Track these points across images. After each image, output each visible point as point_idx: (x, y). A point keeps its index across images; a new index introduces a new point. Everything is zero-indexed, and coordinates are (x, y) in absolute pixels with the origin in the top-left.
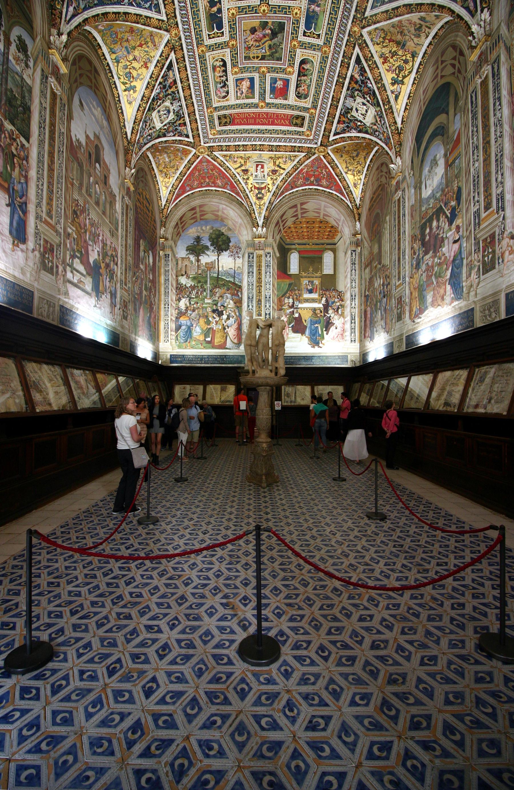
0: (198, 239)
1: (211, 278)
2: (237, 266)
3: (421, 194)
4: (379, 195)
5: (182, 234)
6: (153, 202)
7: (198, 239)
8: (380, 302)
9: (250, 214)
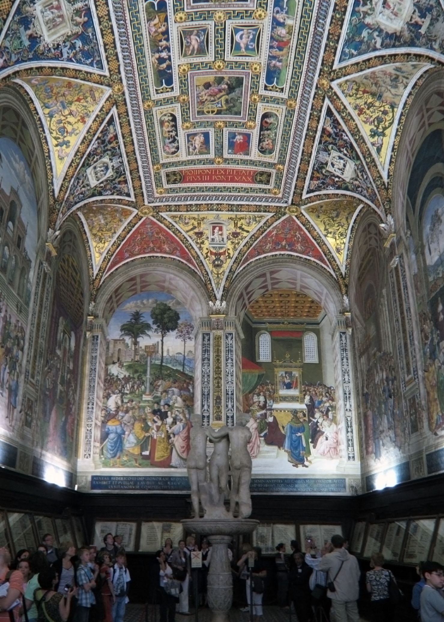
1: (153, 366)
2: (187, 351)
4: (369, 261)
5: (117, 310)
7: (137, 316)
8: (385, 403)
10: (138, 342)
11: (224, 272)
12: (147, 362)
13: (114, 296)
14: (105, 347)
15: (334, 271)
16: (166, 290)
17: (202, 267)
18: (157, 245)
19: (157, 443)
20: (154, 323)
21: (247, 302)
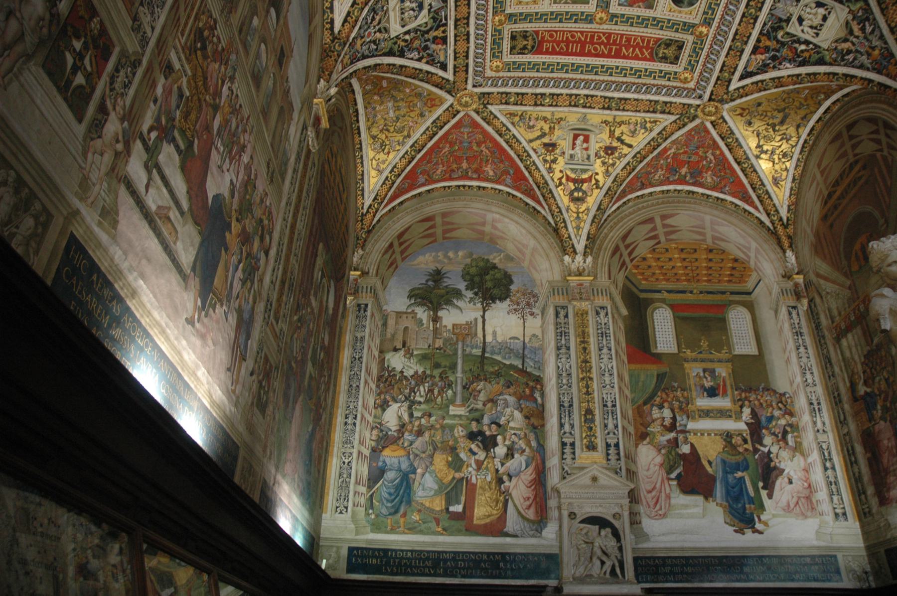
0: (437, 276)
1: (467, 357)
2: (529, 333)
7: (437, 276)
11: (588, 209)
12: (456, 350)
13: (396, 244)
14: (380, 324)
15: (768, 215)
16: (488, 237)
17: (552, 201)
19: (478, 491)
21: (627, 260)
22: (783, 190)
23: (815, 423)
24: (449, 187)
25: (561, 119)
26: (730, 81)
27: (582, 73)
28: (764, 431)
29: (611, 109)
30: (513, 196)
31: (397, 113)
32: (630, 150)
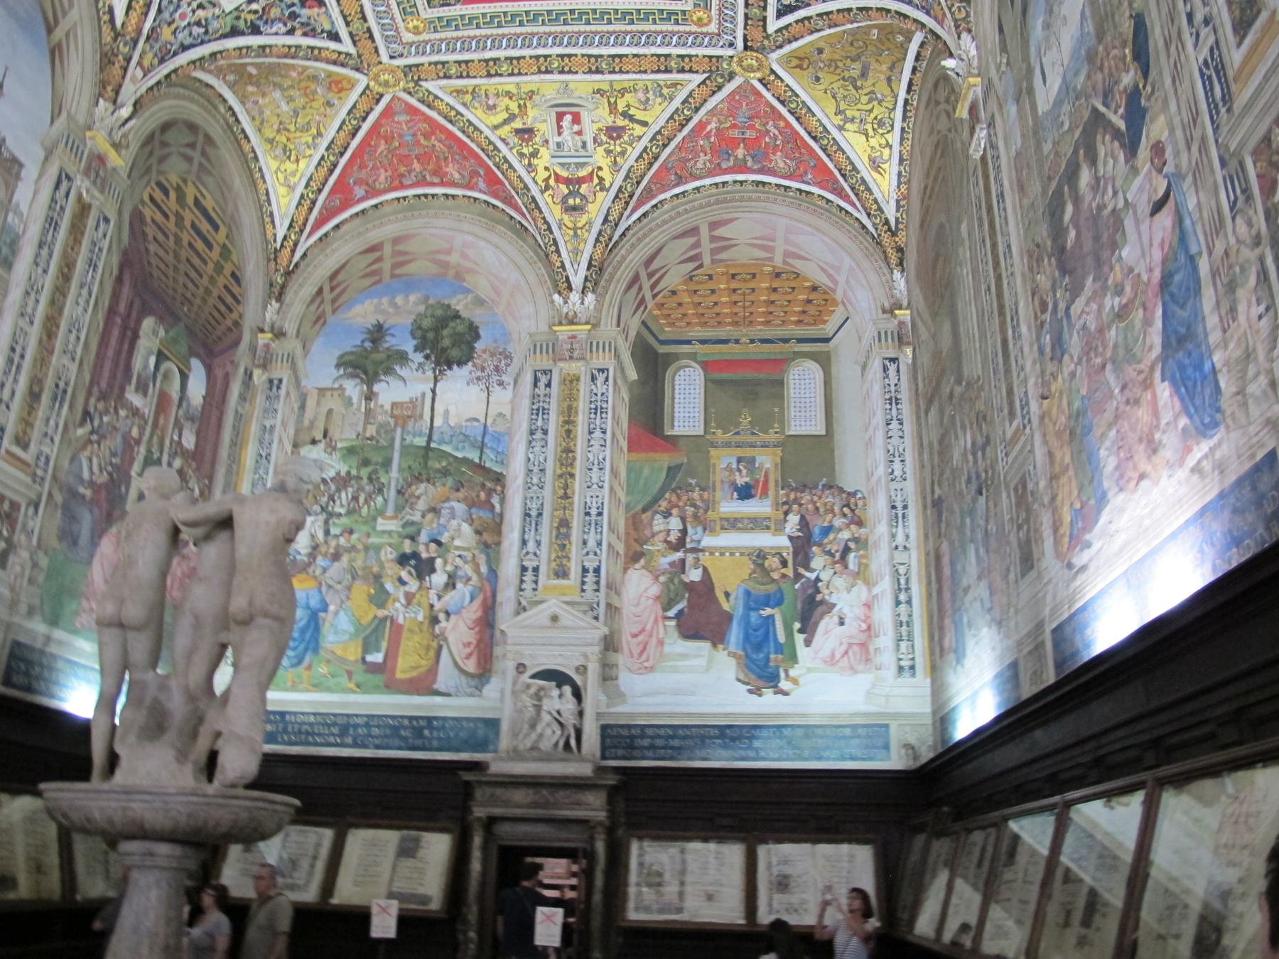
2: (493, 411)
3: (1034, 107)
5: (331, 319)
6: (233, 225)
7: (378, 333)
9: (547, 254)
10: (376, 395)
12: (393, 440)
14: (296, 406)
15: (869, 215)
16: (452, 272)
18: (431, 167)
19: (405, 634)
20: (417, 349)
21: (648, 296)
22: (887, 176)
23: (893, 536)
24: (404, 198)
25: (533, 92)
26: (764, 19)
27: (543, 23)
28: (814, 549)
29: (602, 73)
30: (494, 206)
31: (292, 105)
32: (645, 129)
